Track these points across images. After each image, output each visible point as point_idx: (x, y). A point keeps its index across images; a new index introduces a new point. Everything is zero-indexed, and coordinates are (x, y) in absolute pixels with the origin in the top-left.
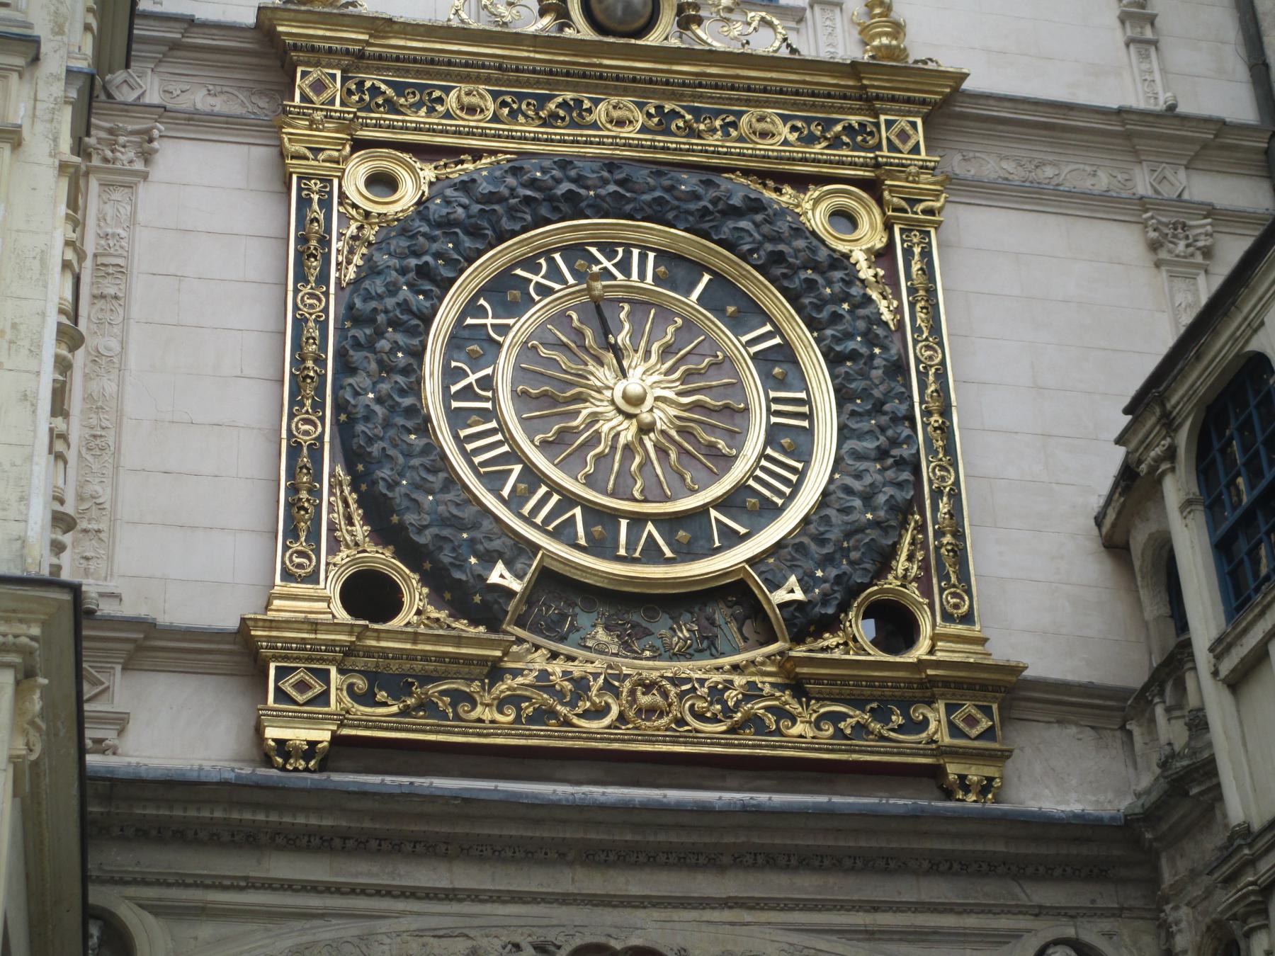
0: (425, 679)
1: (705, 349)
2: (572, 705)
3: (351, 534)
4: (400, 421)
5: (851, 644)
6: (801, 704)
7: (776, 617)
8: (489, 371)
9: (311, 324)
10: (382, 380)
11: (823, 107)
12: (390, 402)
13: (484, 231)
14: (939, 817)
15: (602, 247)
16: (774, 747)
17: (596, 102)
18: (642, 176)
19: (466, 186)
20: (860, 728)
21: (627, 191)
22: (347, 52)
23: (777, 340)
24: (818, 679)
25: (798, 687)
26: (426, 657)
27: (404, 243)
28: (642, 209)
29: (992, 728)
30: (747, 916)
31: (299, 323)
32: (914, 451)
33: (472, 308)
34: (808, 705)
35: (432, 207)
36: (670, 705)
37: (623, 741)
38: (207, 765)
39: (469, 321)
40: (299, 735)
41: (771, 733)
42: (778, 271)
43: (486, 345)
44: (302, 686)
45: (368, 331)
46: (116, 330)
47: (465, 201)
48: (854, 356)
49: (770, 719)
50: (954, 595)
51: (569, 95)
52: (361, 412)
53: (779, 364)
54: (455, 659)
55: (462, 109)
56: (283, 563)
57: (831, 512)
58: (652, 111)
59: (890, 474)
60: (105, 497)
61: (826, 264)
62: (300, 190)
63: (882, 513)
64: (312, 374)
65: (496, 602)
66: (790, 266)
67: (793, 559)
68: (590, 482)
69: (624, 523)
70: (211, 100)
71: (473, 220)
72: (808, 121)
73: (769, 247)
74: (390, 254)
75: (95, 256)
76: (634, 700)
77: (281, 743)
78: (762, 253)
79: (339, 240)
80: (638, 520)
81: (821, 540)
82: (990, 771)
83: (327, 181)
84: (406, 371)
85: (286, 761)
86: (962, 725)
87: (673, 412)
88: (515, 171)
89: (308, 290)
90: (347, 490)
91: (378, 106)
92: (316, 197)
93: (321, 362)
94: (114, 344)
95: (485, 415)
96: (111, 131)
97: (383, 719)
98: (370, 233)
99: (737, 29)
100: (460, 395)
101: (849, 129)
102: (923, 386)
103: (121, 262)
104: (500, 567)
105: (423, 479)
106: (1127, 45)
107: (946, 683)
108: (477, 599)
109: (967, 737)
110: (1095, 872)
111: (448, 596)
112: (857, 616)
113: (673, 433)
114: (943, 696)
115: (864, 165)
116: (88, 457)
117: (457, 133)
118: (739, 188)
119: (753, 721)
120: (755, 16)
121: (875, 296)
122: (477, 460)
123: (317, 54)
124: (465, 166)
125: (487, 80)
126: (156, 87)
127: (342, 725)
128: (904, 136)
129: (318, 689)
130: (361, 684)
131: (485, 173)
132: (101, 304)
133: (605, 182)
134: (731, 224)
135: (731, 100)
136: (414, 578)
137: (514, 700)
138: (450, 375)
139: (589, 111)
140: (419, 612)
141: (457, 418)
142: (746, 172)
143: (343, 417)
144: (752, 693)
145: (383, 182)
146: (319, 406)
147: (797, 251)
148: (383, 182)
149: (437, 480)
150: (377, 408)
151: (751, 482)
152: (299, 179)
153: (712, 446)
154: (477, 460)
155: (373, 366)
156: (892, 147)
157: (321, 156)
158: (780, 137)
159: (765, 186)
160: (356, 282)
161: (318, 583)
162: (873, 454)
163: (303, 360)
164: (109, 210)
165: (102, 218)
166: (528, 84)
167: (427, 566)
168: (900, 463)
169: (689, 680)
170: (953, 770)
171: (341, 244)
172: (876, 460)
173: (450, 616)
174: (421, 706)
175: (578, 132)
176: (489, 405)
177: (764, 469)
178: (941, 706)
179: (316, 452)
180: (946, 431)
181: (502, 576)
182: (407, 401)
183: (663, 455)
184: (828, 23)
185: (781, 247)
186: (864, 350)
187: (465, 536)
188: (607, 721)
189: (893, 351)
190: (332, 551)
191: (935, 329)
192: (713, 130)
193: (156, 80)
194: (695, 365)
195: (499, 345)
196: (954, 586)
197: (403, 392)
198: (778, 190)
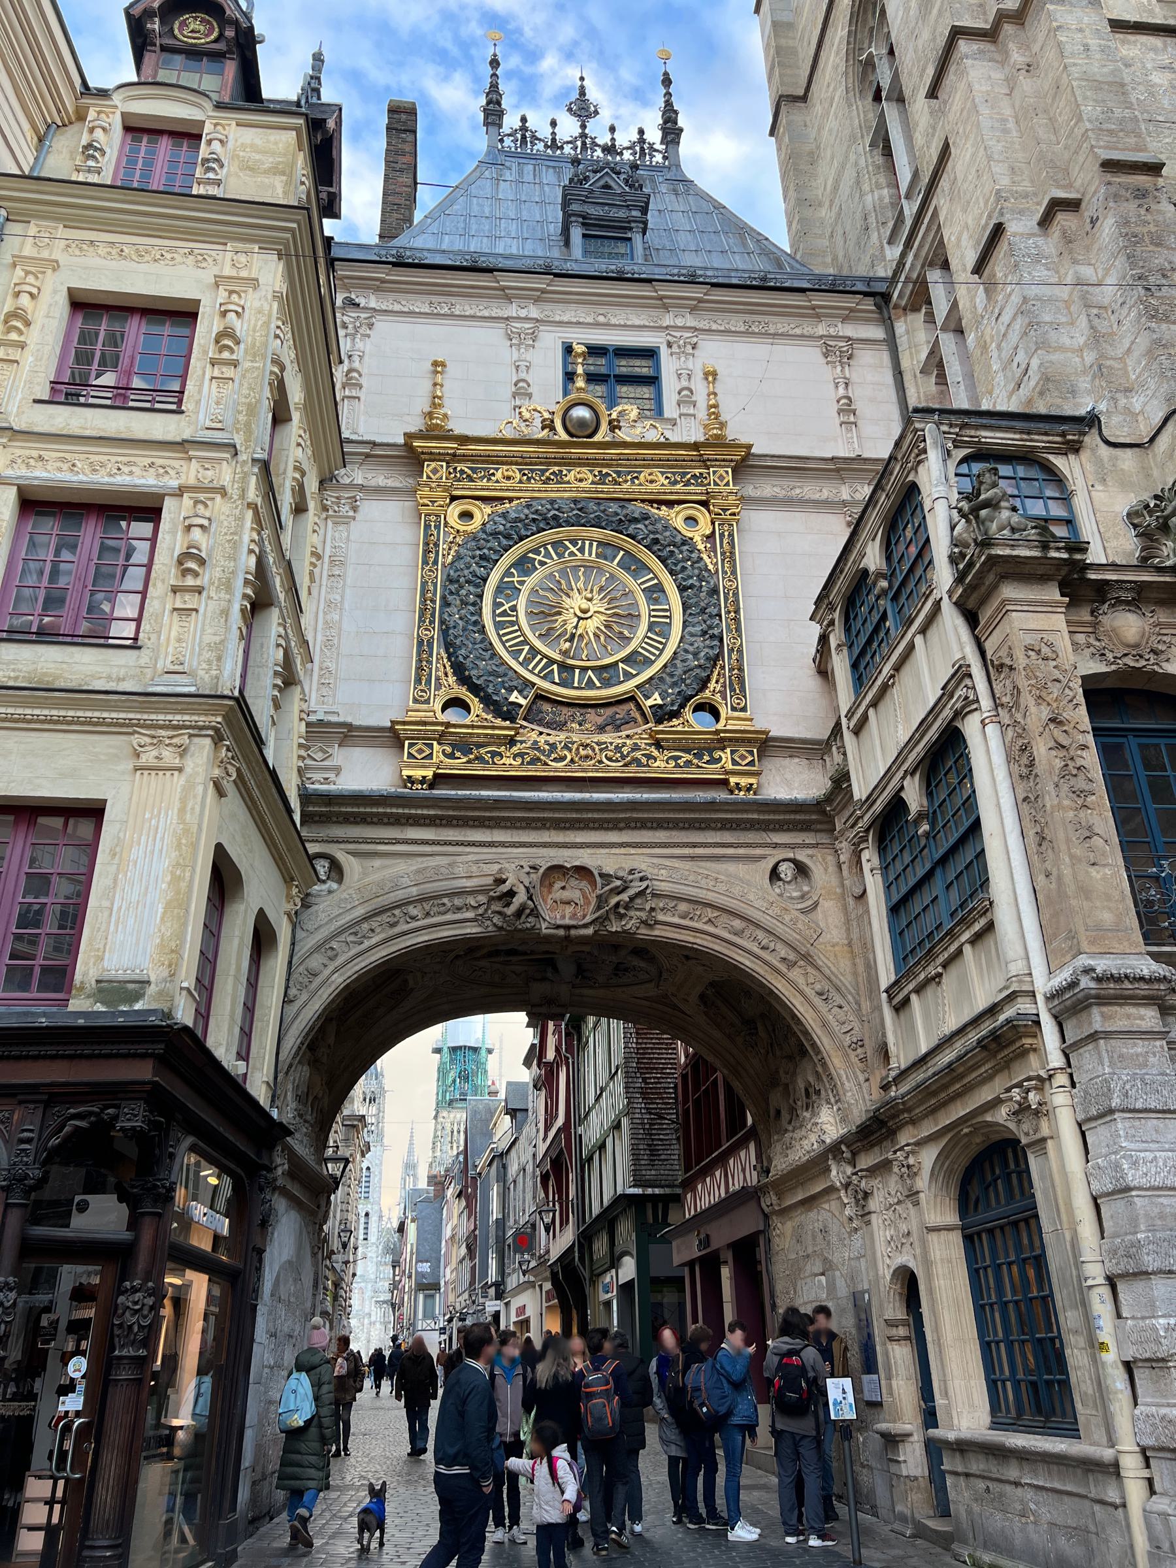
0: (480, 746)
7: (648, 711)
11: (682, 467)
14: (726, 803)
15: (571, 542)
18: (592, 506)
19: (504, 515)
21: (583, 514)
24: (667, 740)
25: (658, 745)
26: (478, 735)
30: (633, 851)
31: (424, 584)
33: (507, 573)
40: (418, 773)
42: (655, 548)
44: (420, 751)
48: (691, 587)
49: (644, 760)
52: (452, 624)
53: (655, 592)
54: (492, 736)
57: (677, 662)
60: (333, 667)
77: (409, 777)
80: (584, 669)
81: (671, 675)
83: (438, 516)
84: (474, 604)
87: (603, 618)
88: (528, 506)
94: (338, 597)
95: (512, 623)
97: (458, 765)
99: (638, 431)
100: (500, 615)
102: (726, 599)
107: (730, 739)
110: (805, 827)
118: (637, 508)
119: (636, 761)
120: (648, 423)
121: (705, 556)
123: (434, 457)
125: (517, 464)
128: (721, 478)
130: (449, 749)
135: (636, 466)
137: (521, 755)
138: (496, 605)
141: (498, 626)
142: (643, 501)
144: (636, 748)
145: (466, 515)
146: (432, 622)
148: (466, 515)
149: (487, 655)
156: (716, 484)
158: (657, 481)
165: (333, 539)
168: (712, 637)
170: (733, 780)
174: (477, 758)
178: (728, 750)
179: (430, 645)
180: (737, 620)
191: (734, 572)
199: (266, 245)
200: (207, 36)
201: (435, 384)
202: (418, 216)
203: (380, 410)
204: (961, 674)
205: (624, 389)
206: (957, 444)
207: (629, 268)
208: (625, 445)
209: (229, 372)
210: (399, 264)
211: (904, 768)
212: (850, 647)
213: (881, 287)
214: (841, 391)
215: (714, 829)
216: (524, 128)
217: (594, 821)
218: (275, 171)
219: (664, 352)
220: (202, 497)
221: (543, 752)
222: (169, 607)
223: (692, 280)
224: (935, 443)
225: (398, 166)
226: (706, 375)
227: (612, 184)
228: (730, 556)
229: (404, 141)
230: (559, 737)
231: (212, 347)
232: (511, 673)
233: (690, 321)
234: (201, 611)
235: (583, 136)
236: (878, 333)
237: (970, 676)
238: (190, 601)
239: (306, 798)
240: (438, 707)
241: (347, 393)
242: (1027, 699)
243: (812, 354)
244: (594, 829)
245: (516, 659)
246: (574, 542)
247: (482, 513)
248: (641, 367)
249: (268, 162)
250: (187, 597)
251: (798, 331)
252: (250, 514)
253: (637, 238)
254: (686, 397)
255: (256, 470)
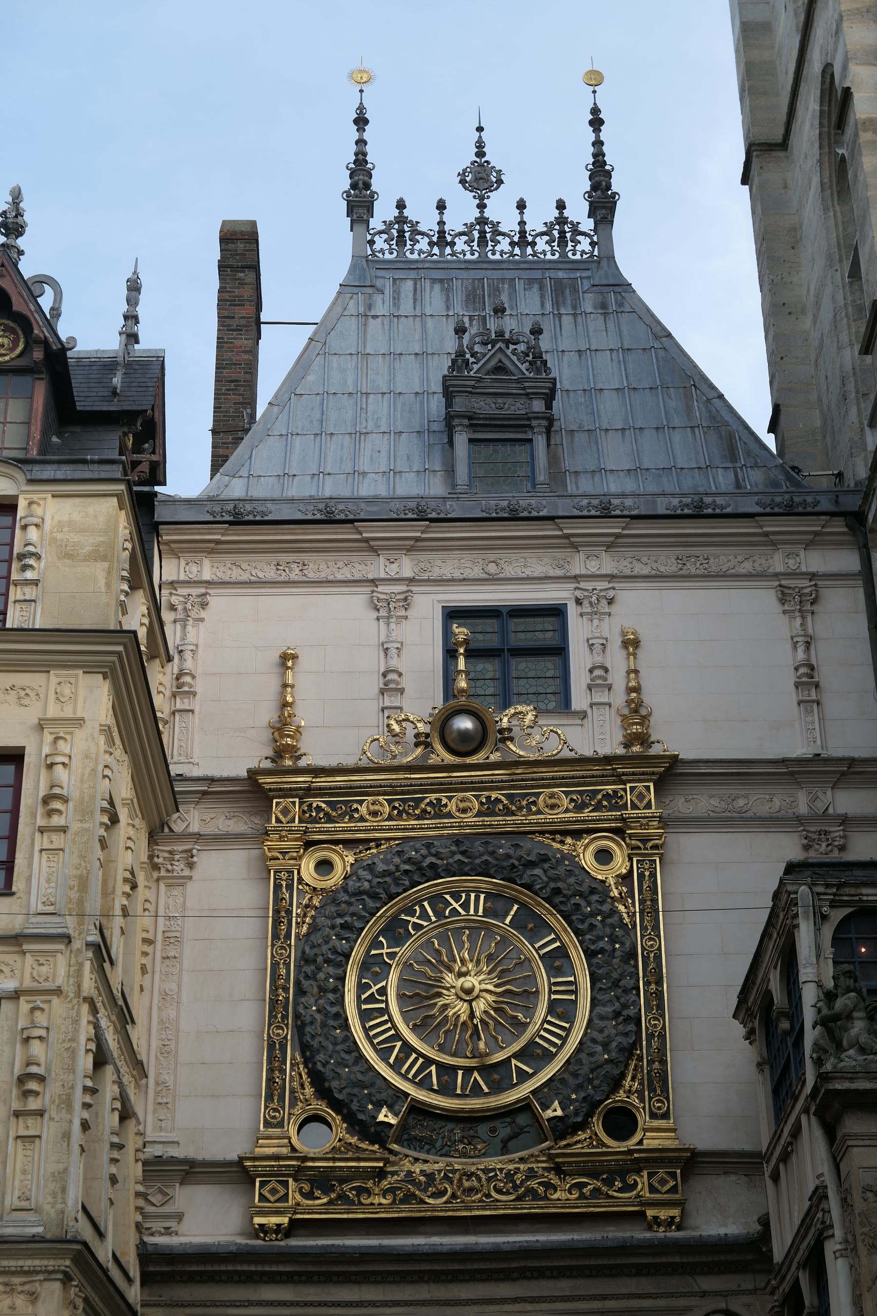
0: (342, 1181)
1: (514, 955)
2: (425, 1190)
3: (303, 1094)
4: (331, 1022)
5: (594, 1137)
6: (560, 1178)
8: (384, 983)
9: (281, 966)
10: (320, 997)
12: (325, 1011)
13: (380, 895)
16: (542, 1208)
17: (450, 798)
19: (370, 868)
20: (596, 1192)
21: (468, 856)
22: (300, 789)
23: (558, 944)
25: (558, 1170)
27: (333, 909)
28: (475, 869)
29: (676, 1185)
30: (529, 1307)
31: (275, 966)
32: (636, 1011)
34: (564, 1179)
35: (351, 883)
36: (482, 1186)
37: (454, 1210)
38: (223, 1239)
39: (373, 952)
40: (274, 1220)
41: (542, 1199)
42: (558, 899)
43: (382, 966)
44: (273, 1191)
45: (313, 967)
46: (175, 978)
47: (369, 877)
48: (602, 951)
50: (659, 1101)
51: (433, 796)
52: (308, 1019)
53: (557, 961)
55: (369, 814)
56: (265, 1116)
57: (583, 1056)
58: (484, 800)
59: (621, 1027)
60: (170, 1083)
61: (587, 892)
62: (275, 879)
63: (613, 1054)
64: (281, 998)
65: (383, 1131)
66: (564, 896)
67: (558, 1089)
68: (442, 1049)
69: (460, 1072)
70: (228, 822)
71: (373, 889)
72: (581, 793)
73: (552, 885)
74: (325, 916)
75: (164, 932)
76: (462, 1184)
77: (262, 1226)
78: (548, 889)
79: (298, 907)
81: (575, 1075)
82: (675, 1212)
84: (335, 990)
85: (265, 1236)
86: (657, 1185)
87: (490, 998)
88: (399, 853)
89: (279, 944)
90: (301, 1067)
91: (320, 818)
92: (284, 883)
93: (286, 989)
94: (174, 987)
96: (170, 852)
97: (318, 1208)
98: (316, 902)
101: (607, 796)
103: (177, 934)
104: (384, 1110)
105: (343, 1059)
106: (799, 704)
107: (646, 1160)
108: (373, 1129)
109: (660, 1192)
111: (357, 1128)
112: (598, 1120)
113: (492, 1012)
114: (646, 1168)
115: (615, 820)
116: (162, 1059)
117: (366, 830)
121: (621, 908)
122: (375, 1041)
124: (372, 851)
126: (196, 817)
127: (295, 1213)
128: (641, 797)
129: (282, 1193)
130: (307, 1187)
131: (382, 857)
132: (167, 962)
133: (453, 853)
134: (529, 872)
135: (533, 787)
136: (338, 1118)
137: (392, 1190)
138: (362, 988)
139: (446, 805)
140: (340, 1140)
141: (365, 1016)
142: (542, 833)
143: (299, 1023)
144: (531, 1174)
146: (285, 1017)
147: (569, 885)
148: (325, 866)
149: (350, 1058)
150: (318, 1017)
151: (537, 1040)
152: (275, 872)
153: (516, 1017)
154: (375, 1041)
155: (316, 990)
156: (634, 806)
157: (287, 857)
159: (554, 840)
160: (308, 934)
161: (283, 1127)
162: (611, 1016)
163: (277, 989)
164: (171, 901)
166: (408, 793)
167: (345, 1111)
169: (494, 1170)
170: (650, 1213)
171: (299, 911)
172: (613, 1019)
173: (359, 1139)
174: (339, 1197)
175: (438, 821)
176: (383, 1005)
177: (546, 1030)
178: (645, 1174)
180: (659, 995)
181: (385, 1116)
182: (334, 1010)
183: (485, 1026)
184: (601, 718)
185: (560, 885)
186: (608, 947)
187: (366, 1092)
188: (444, 1199)
189: (627, 945)
190: (292, 1105)
191: (656, 928)
192: (520, 808)
193: (196, 812)
194: (505, 966)
195: (390, 966)
196: (659, 1095)
197: (332, 1004)
198: (562, 842)
199: (89, 669)
200: (11, 350)
201: (285, 686)
202: (261, 408)
203: (214, 742)
204: (819, 1195)
205: (522, 666)
206: (834, 905)
207: (527, 502)
208: (517, 764)
209: (58, 840)
210: (236, 522)
211: (796, 1260)
212: (771, 1067)
213: (852, 503)
214: (801, 655)
215: (628, 1275)
216: (401, 220)
217: (481, 1271)
218: (97, 555)
219: (572, 611)
220: (39, 1000)
221: (418, 1185)
222: (12, 1134)
223: (606, 513)
224: (806, 913)
225: (234, 323)
226: (626, 644)
227: (507, 363)
228: (650, 909)
229: (242, 284)
230: (438, 1165)
231: (40, 810)
232: (379, 1082)
233: (607, 564)
234: (44, 1137)
235: (482, 221)
236: (847, 560)
237: (827, 1197)
238: (31, 1126)
239: (148, 1256)
240: (292, 1131)
241: (179, 706)
242: (862, 1250)
243: (763, 600)
244: (479, 1280)
245: (386, 1060)
246: (456, 896)
247: (343, 862)
248: (541, 633)
249: (88, 543)
250: (30, 1121)
251: (746, 567)
252: (85, 1008)
253: (540, 442)
254: (599, 678)
255: (90, 954)
